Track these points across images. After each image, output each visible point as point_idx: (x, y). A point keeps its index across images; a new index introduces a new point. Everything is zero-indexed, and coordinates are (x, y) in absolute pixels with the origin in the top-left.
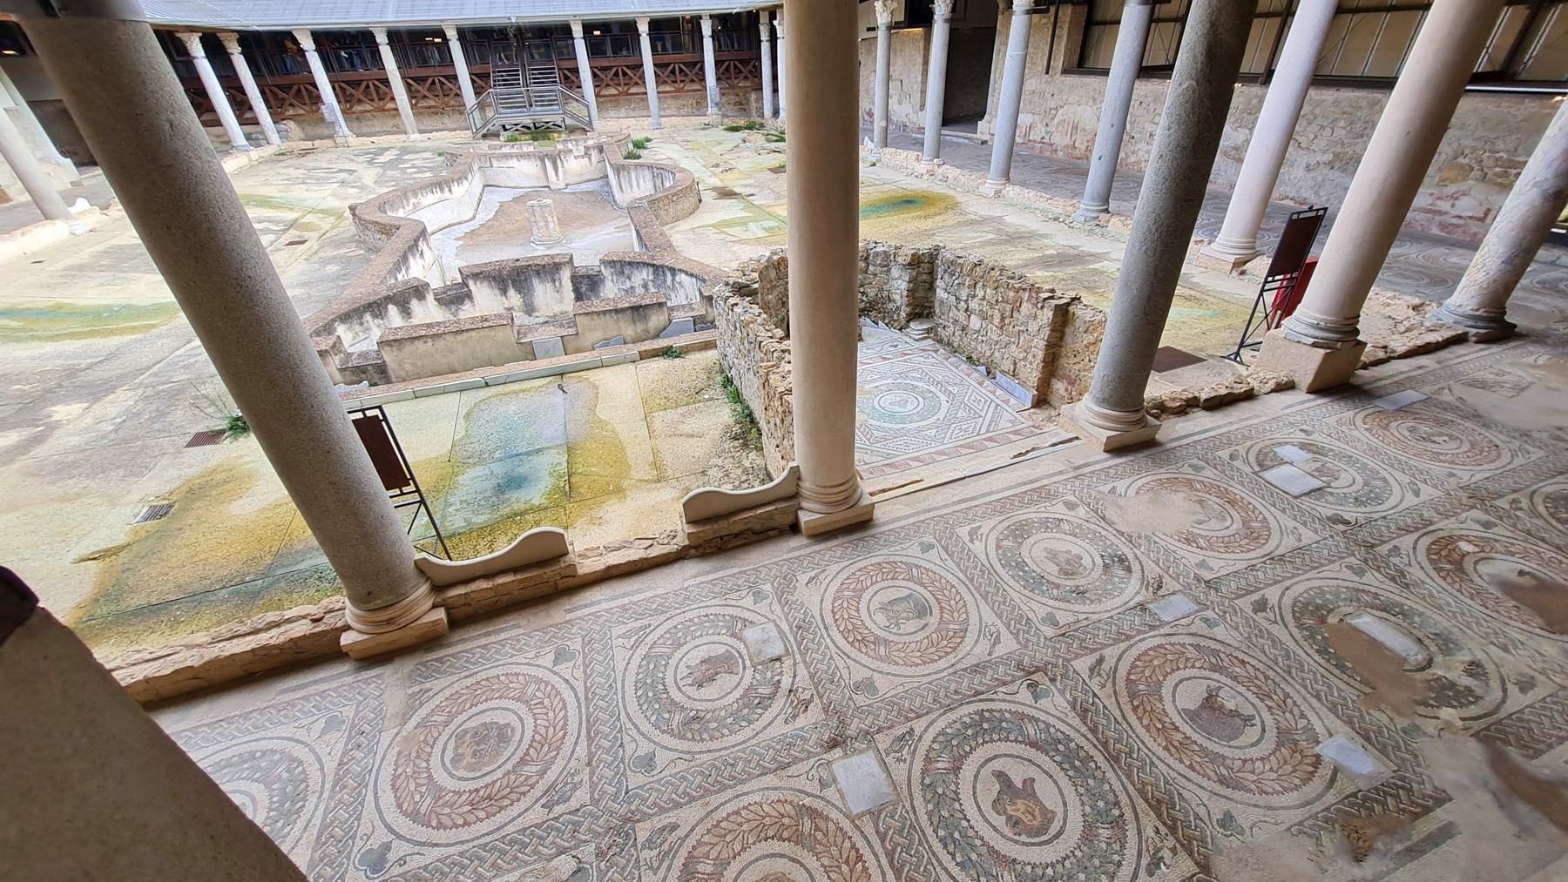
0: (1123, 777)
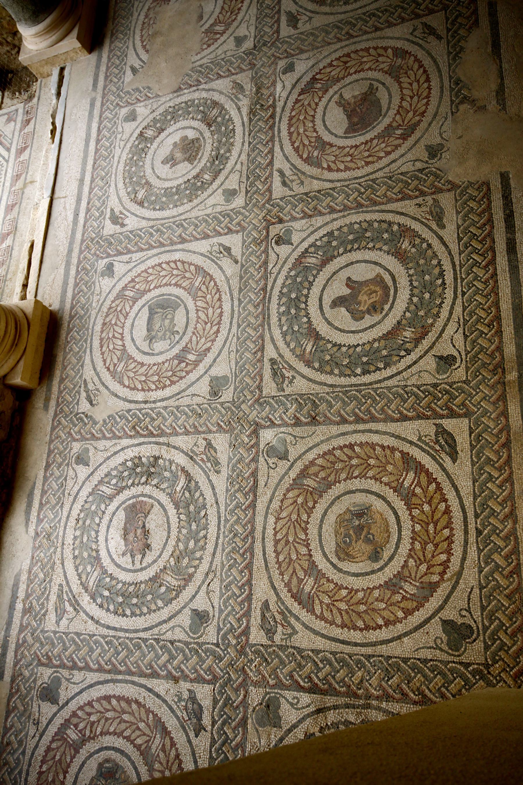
0: (374, 208)
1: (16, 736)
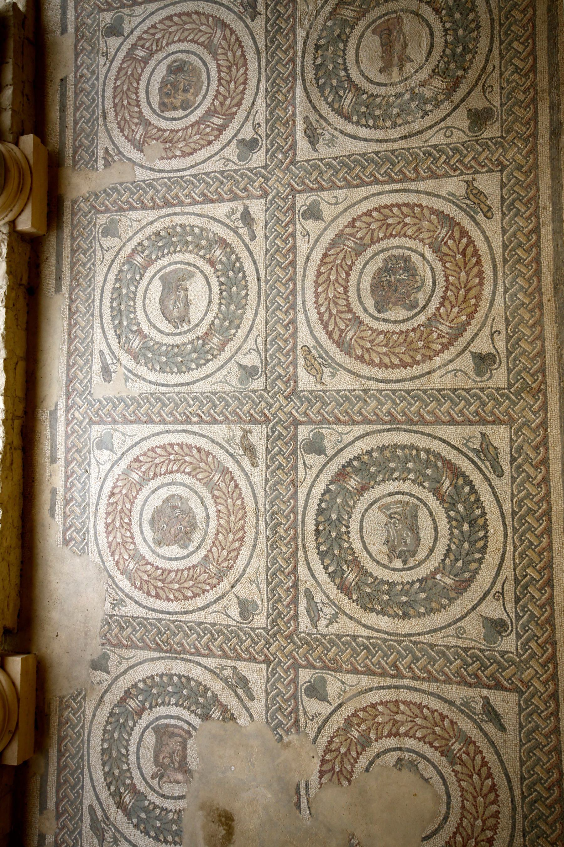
1: (88, 69)
